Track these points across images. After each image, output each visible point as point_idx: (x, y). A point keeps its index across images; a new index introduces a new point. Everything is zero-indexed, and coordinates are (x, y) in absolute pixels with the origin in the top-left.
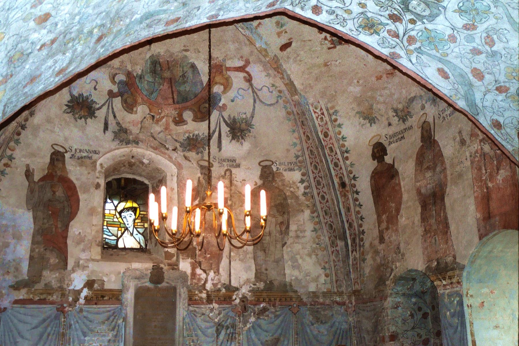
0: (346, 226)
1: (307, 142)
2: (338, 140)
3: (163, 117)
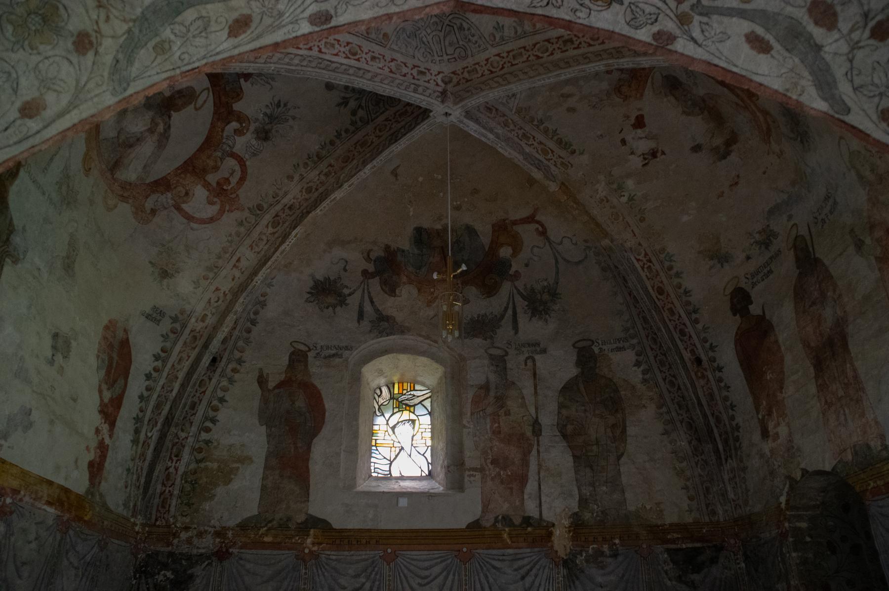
0: (712, 421)
2: (680, 297)
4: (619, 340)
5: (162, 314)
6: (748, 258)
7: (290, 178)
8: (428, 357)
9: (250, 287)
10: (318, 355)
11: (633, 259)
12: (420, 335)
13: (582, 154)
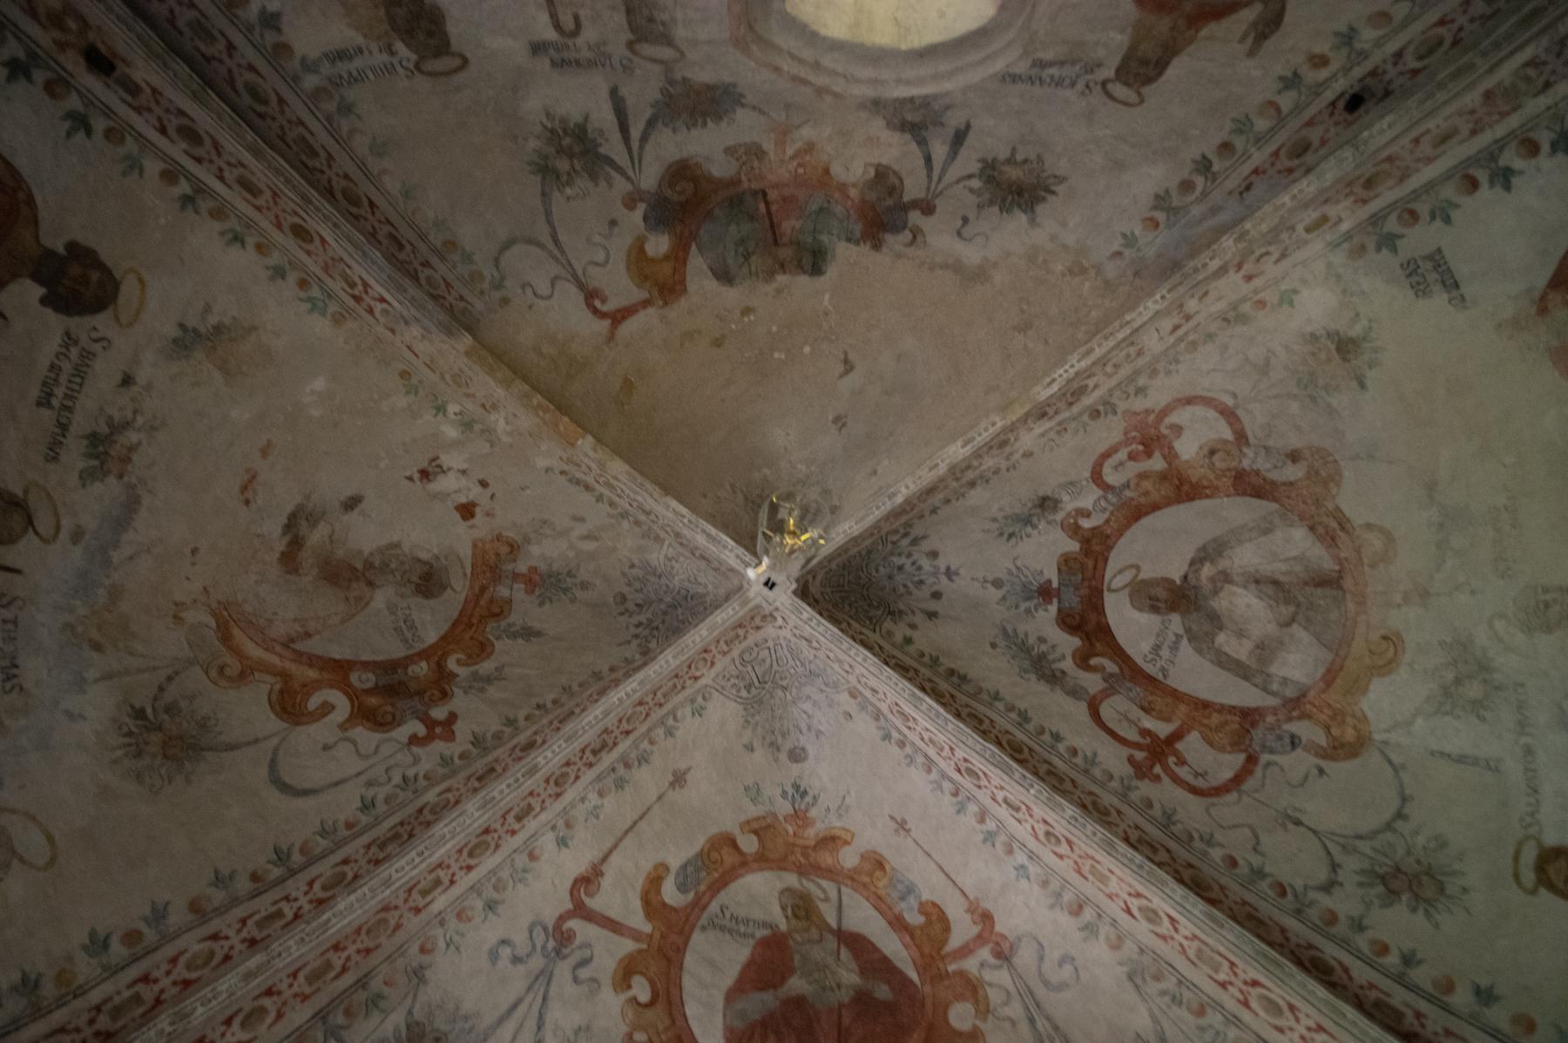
1: (346, 177)
3: (792, 158)
4: (356, 79)
5: (1411, 269)
6: (127, 381)
7: (1028, 455)
8: (825, 39)
11: (395, 304)
12: (836, 95)
13: (547, 470)
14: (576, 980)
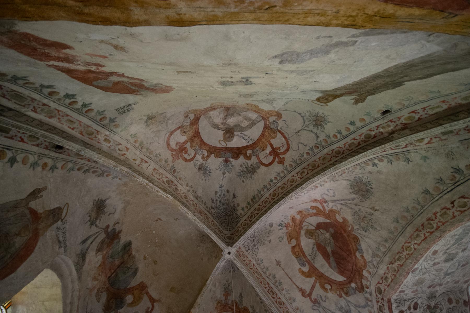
9: (135, 175)
10: (58, 229)
14: (325, 301)
